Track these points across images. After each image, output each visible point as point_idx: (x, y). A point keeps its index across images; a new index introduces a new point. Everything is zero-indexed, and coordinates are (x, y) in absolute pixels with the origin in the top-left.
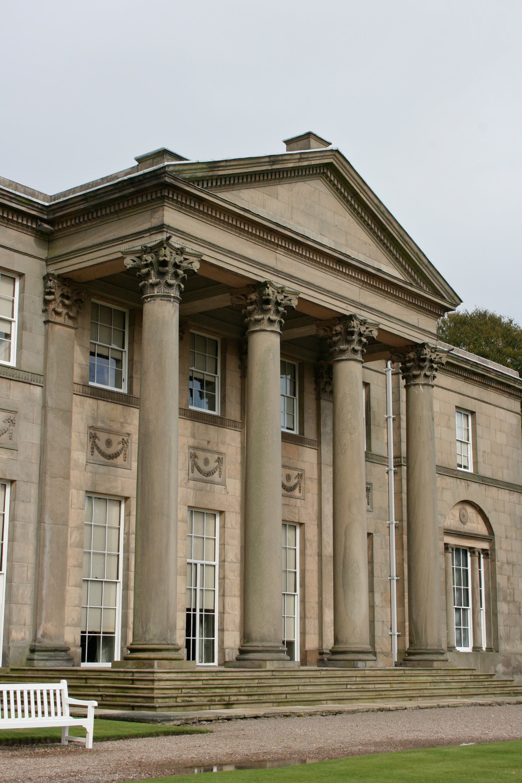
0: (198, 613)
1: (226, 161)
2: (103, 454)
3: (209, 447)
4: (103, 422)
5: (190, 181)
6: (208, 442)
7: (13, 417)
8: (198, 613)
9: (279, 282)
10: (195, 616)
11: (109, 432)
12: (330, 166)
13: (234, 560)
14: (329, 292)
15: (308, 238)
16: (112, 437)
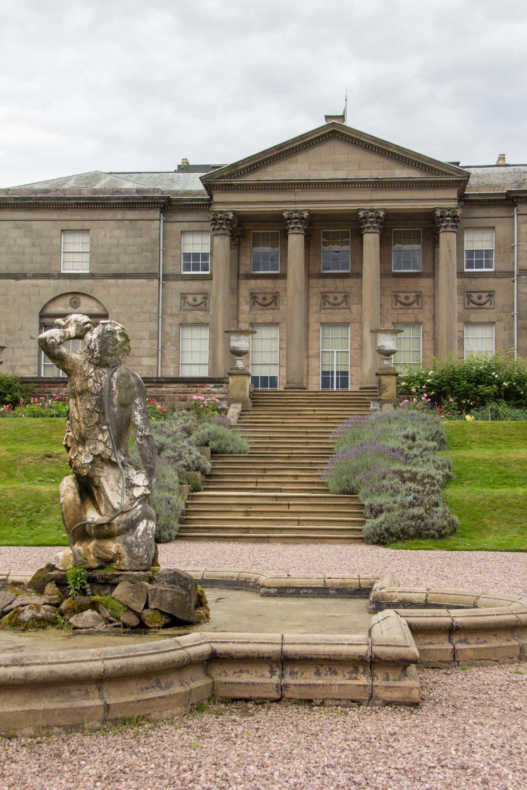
0: (335, 376)
1: (242, 161)
2: (261, 305)
3: (337, 290)
4: (260, 289)
5: (230, 176)
6: (336, 288)
7: (206, 296)
8: (335, 376)
9: (292, 207)
10: (333, 378)
11: (265, 293)
12: (334, 131)
13: (357, 347)
14: (339, 201)
15: (310, 180)
16: (267, 296)
